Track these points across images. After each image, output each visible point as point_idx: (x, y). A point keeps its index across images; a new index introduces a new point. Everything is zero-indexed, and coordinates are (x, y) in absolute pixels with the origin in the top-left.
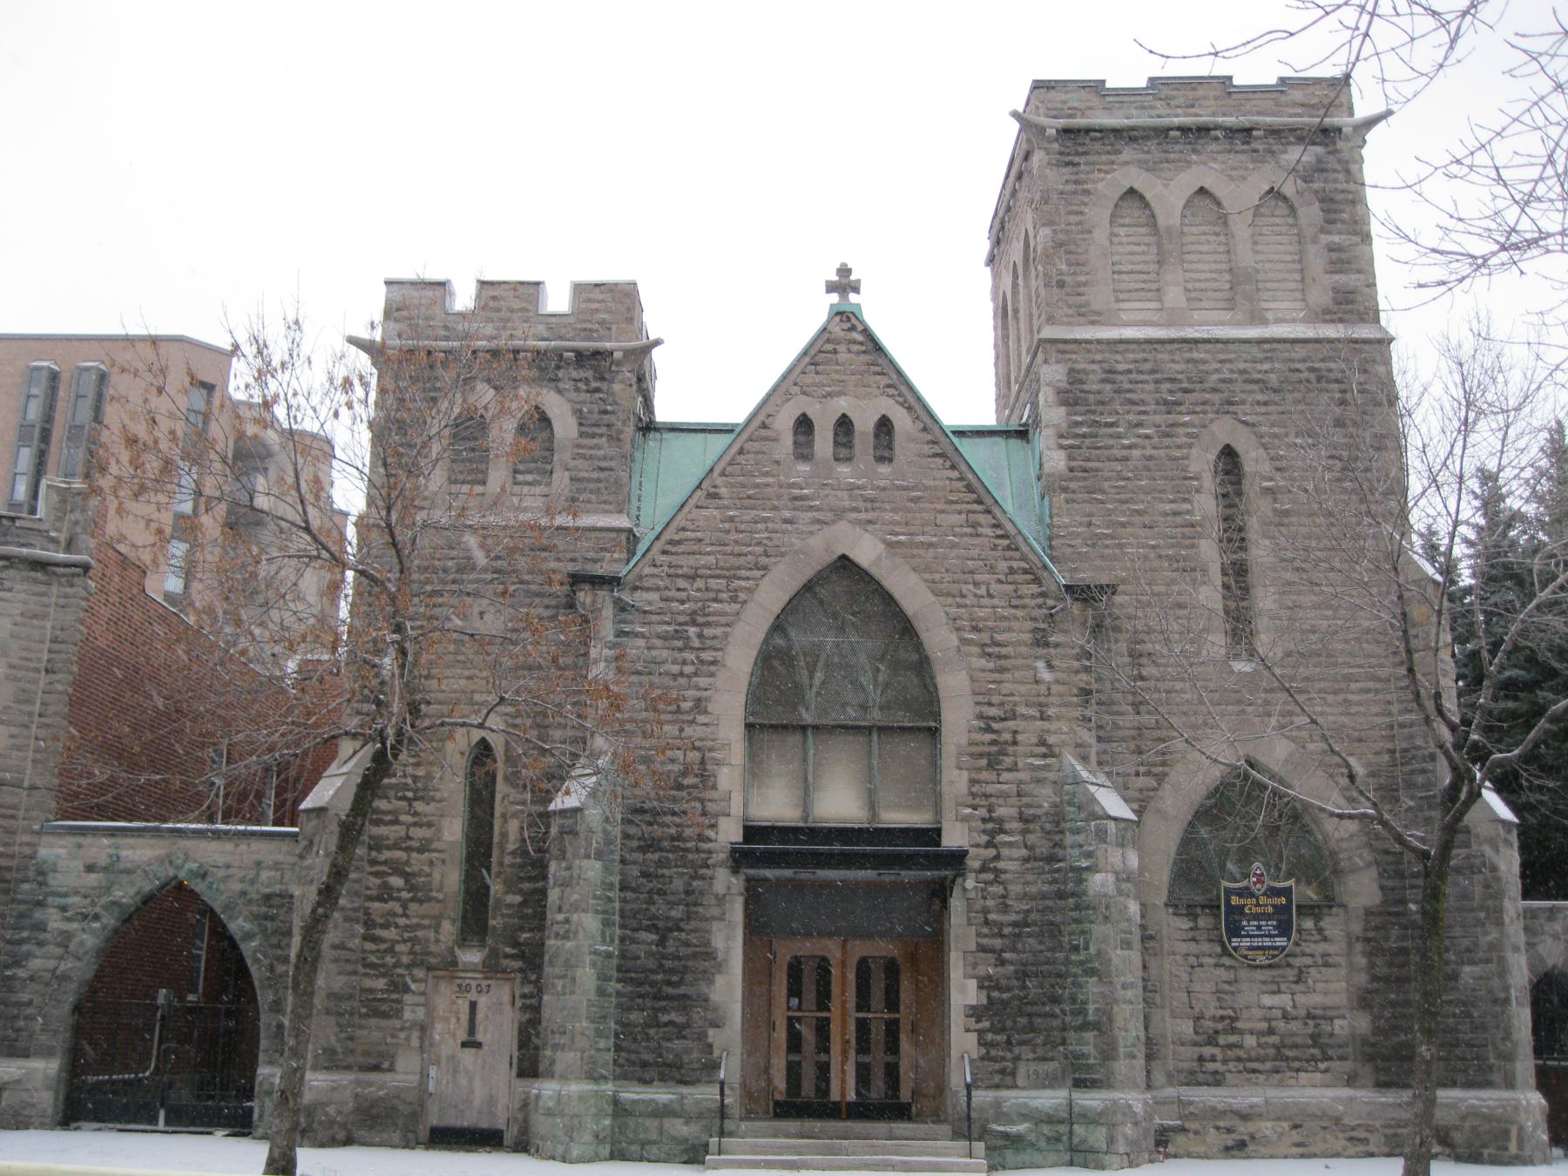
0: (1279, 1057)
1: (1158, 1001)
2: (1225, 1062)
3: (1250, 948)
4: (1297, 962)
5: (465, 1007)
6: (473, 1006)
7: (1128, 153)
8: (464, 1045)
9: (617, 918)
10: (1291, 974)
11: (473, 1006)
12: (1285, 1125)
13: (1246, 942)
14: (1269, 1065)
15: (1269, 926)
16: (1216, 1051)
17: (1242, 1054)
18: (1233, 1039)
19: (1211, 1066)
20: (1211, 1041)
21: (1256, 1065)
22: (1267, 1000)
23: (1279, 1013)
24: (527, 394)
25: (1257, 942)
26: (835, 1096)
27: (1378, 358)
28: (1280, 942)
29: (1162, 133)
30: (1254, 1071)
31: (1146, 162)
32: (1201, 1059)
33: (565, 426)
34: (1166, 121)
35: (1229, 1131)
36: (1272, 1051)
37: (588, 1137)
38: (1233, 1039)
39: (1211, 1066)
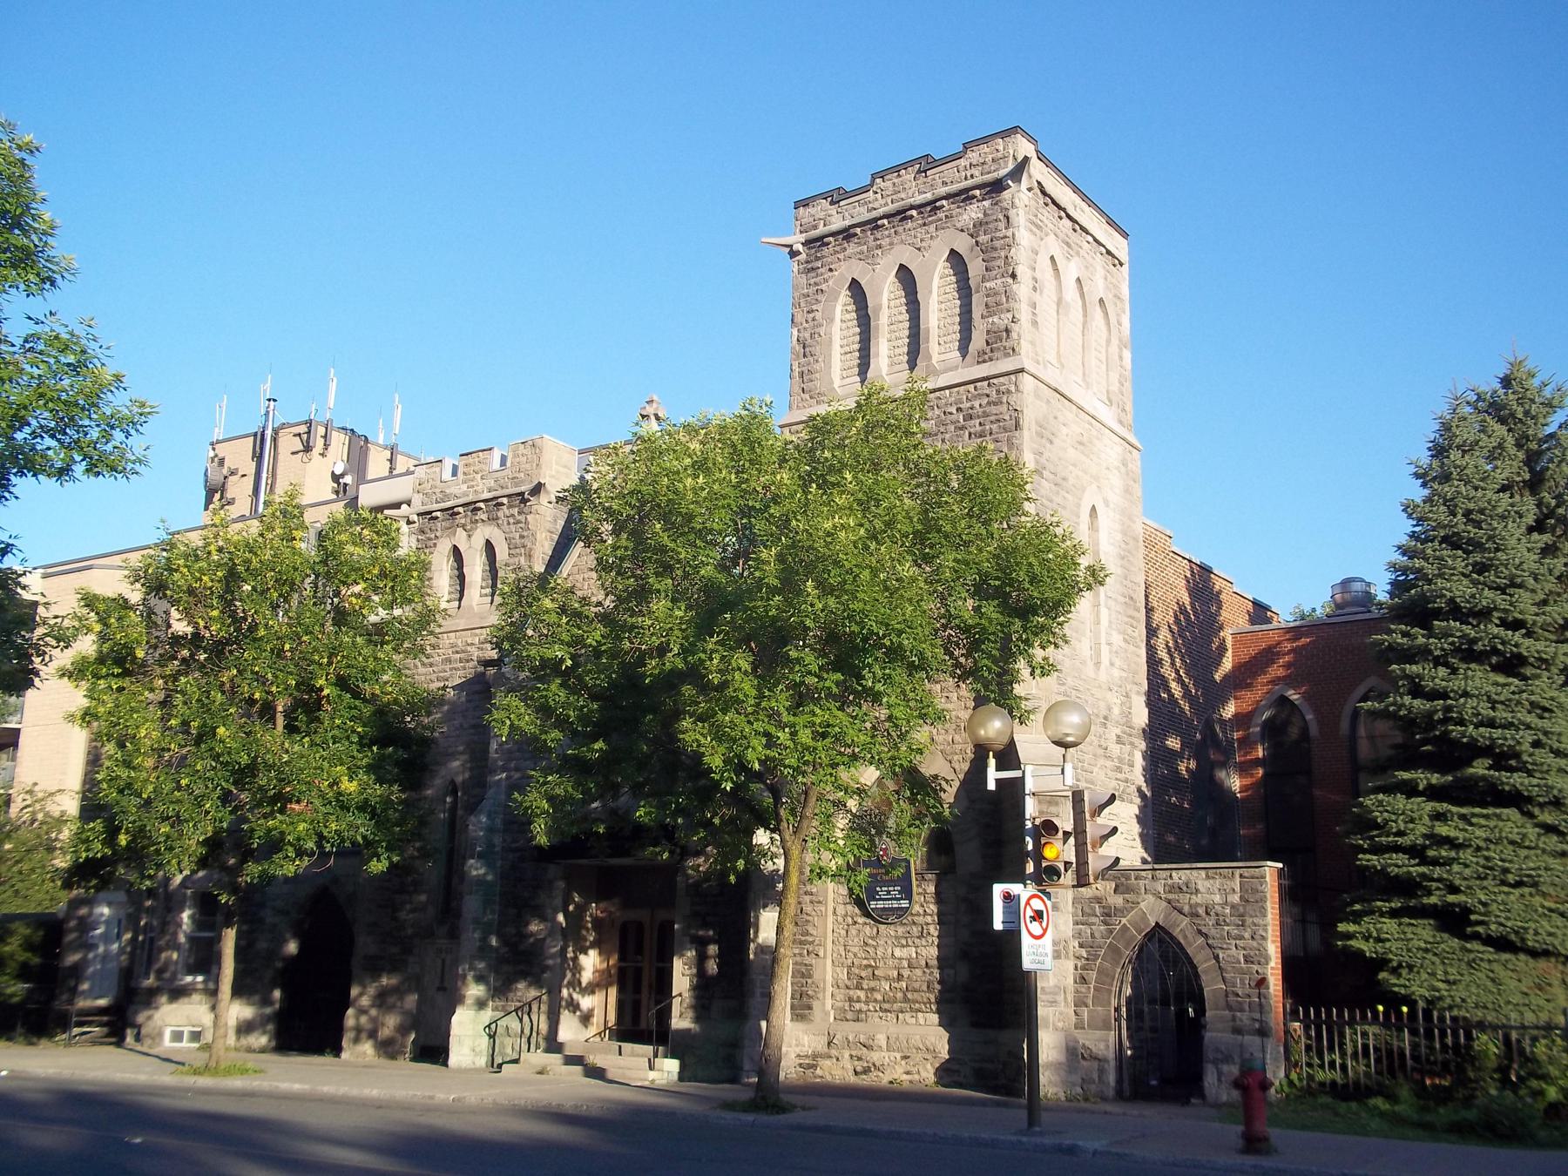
0: (906, 1000)
1: (821, 954)
2: (867, 1003)
3: (884, 909)
4: (920, 920)
5: (439, 962)
6: (443, 961)
7: (852, 248)
8: (439, 989)
9: (497, 898)
10: (915, 930)
11: (443, 961)
12: (898, 1056)
13: (880, 905)
14: (896, 1006)
15: (895, 891)
16: (862, 994)
17: (879, 997)
18: (873, 984)
19: (857, 1006)
20: (859, 987)
21: (886, 1006)
22: (898, 953)
23: (905, 963)
24: (484, 532)
25: (888, 904)
26: (643, 1025)
27: (1013, 388)
28: (904, 903)
29: (873, 224)
30: (887, 1011)
31: (861, 253)
32: (850, 1000)
33: (502, 554)
34: (874, 214)
35: (859, 1059)
36: (899, 995)
37: (466, 1050)
38: (873, 984)
39: (857, 1006)
